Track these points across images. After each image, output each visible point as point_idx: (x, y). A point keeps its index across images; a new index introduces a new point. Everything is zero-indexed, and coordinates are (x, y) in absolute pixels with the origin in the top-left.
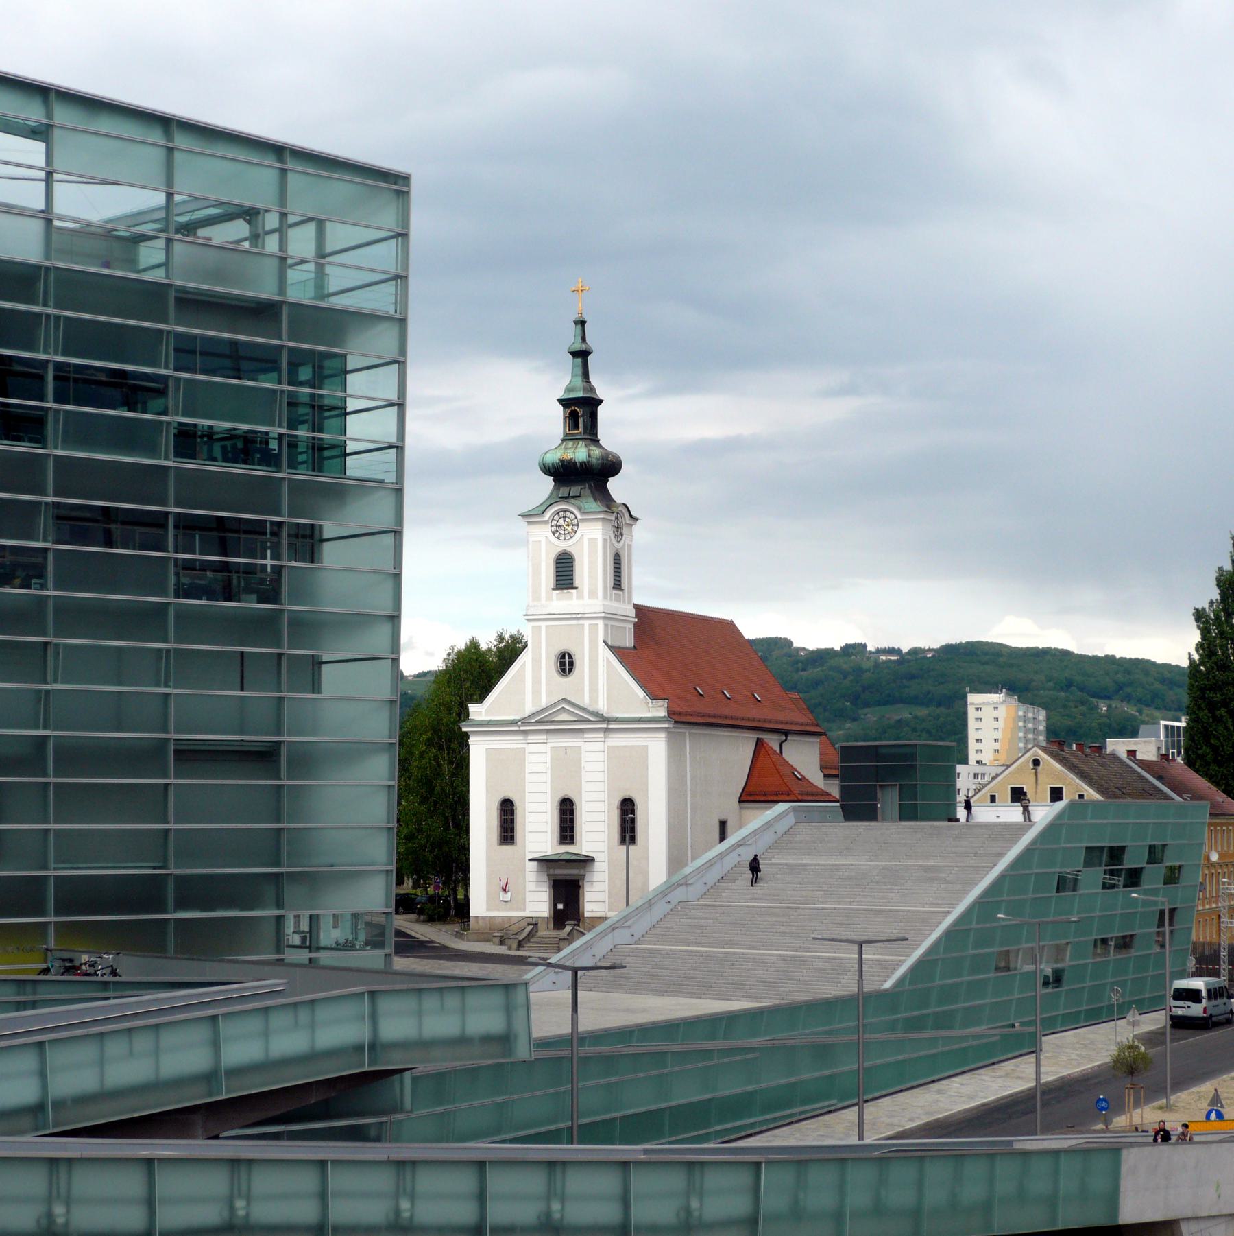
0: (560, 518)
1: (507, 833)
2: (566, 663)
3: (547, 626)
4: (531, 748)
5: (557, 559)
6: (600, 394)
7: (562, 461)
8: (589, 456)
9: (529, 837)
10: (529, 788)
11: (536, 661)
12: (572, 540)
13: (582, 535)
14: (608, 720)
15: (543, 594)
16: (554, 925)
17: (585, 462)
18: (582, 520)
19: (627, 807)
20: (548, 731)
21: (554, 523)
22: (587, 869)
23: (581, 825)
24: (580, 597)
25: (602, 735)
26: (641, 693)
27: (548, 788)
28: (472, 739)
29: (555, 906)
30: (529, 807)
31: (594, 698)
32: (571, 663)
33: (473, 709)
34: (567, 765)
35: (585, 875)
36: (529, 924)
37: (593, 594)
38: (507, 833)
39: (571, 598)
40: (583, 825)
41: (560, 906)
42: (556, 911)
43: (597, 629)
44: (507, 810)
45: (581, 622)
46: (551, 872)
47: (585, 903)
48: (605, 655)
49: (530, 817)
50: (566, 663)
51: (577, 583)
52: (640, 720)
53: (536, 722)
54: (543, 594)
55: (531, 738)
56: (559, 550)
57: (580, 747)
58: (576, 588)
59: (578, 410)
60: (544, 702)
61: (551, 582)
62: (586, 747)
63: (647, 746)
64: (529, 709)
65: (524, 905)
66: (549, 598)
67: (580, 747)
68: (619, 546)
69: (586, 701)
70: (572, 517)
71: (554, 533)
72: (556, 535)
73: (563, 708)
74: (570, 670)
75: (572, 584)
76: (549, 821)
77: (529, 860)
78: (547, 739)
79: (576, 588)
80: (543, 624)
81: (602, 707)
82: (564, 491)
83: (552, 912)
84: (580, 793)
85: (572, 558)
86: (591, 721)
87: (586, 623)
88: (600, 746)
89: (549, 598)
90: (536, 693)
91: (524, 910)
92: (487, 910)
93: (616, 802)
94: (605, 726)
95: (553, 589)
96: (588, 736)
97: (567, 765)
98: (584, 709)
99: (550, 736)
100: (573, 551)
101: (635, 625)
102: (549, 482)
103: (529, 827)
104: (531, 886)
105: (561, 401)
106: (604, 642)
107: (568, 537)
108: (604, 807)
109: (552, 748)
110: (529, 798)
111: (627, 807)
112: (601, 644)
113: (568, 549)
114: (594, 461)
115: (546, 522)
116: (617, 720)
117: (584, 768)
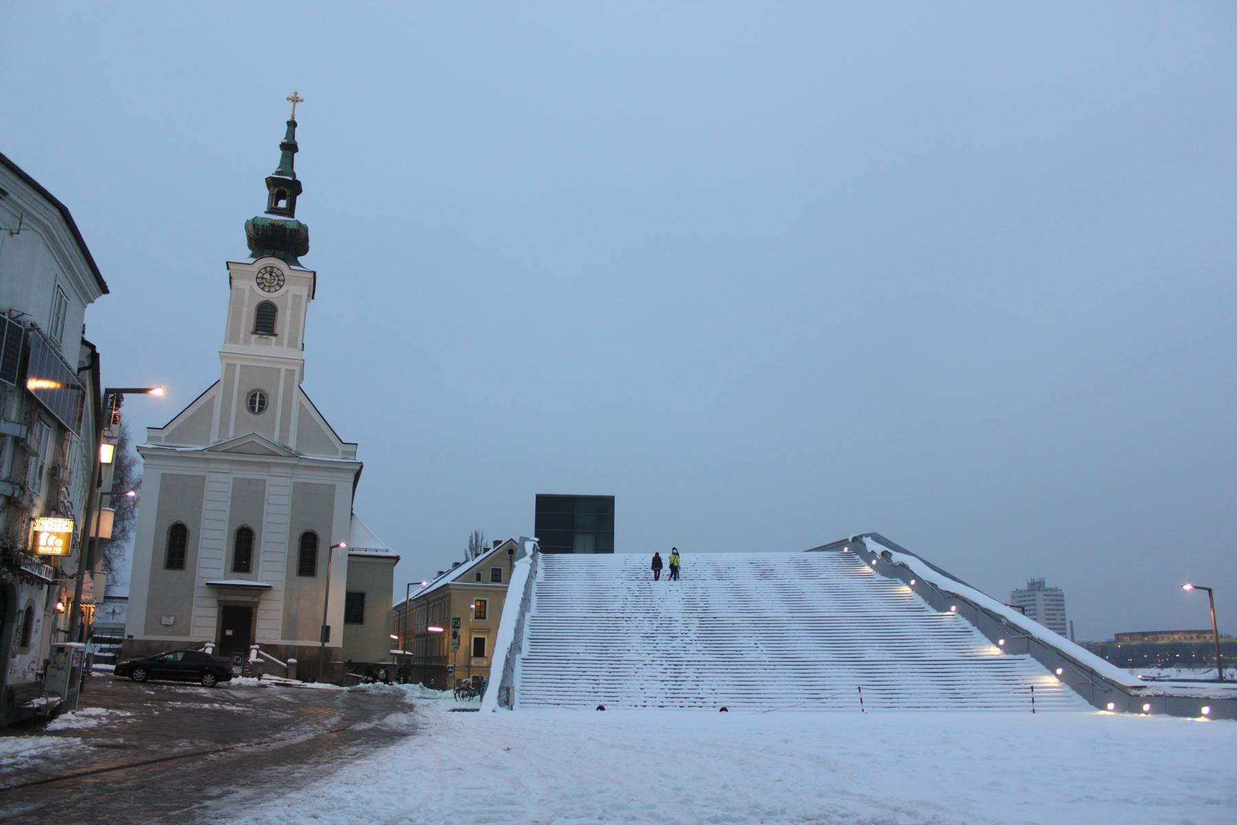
0: (267, 272)
3: (242, 366)
12: (277, 293)
13: (288, 291)
15: (242, 336)
17: (295, 230)
20: (233, 462)
21: (260, 275)
22: (262, 597)
23: (259, 554)
24: (280, 344)
27: (226, 516)
29: (223, 632)
34: (247, 495)
35: (259, 602)
40: (261, 555)
41: (229, 633)
43: (294, 374)
46: (222, 598)
49: (203, 543)
51: (277, 330)
54: (242, 336)
55: (212, 466)
56: (262, 300)
57: (265, 481)
58: (276, 335)
59: (286, 190)
61: (251, 327)
63: (335, 485)
65: (189, 631)
67: (265, 481)
71: (259, 284)
72: (261, 286)
73: (253, 441)
74: (261, 410)
75: (272, 331)
76: (225, 548)
78: (231, 470)
83: (219, 638)
84: (261, 523)
86: (281, 456)
90: (224, 424)
91: (188, 635)
92: (145, 633)
95: (253, 333)
97: (247, 495)
104: (196, 611)
107: (273, 289)
108: (284, 538)
109: (235, 479)
117: (267, 500)
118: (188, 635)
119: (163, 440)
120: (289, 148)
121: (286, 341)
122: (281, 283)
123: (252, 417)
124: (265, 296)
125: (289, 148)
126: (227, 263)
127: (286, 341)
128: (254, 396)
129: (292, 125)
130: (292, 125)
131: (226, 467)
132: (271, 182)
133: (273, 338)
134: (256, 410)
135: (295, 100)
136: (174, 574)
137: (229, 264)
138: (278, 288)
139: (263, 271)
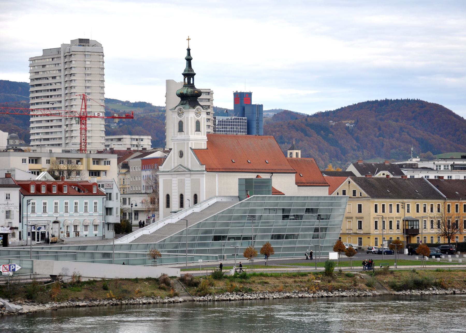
1: (168, 205)
2: (181, 154)
3: (177, 143)
4: (173, 179)
6: (195, 72)
7: (181, 93)
8: (187, 92)
9: (173, 206)
10: (173, 191)
11: (174, 153)
14: (190, 171)
15: (176, 133)
19: (182, 196)
24: (184, 134)
25: (189, 175)
26: (198, 163)
27: (177, 191)
28: (160, 176)
30: (173, 197)
31: (188, 164)
33: (160, 167)
34: (181, 184)
38: (168, 205)
39: (182, 135)
44: (168, 197)
45: (185, 142)
48: (190, 151)
49: (173, 200)
50: (181, 154)
51: (184, 130)
52: (198, 171)
53: (174, 171)
54: (176, 133)
55: (173, 176)
56: (179, 120)
57: (184, 179)
58: (183, 132)
60: (176, 166)
61: (178, 131)
62: (186, 179)
64: (173, 168)
67: (184, 179)
68: (199, 119)
69: (186, 165)
71: (178, 115)
79: (183, 132)
81: (190, 167)
82: (182, 102)
87: (186, 142)
88: (189, 179)
89: (177, 135)
90: (174, 163)
93: (179, 194)
94: (189, 173)
95: (178, 132)
97: (181, 184)
98: (185, 168)
99: (178, 175)
100: (200, 120)
101: (207, 142)
102: (179, 99)
103: (173, 203)
105: (183, 74)
106: (191, 148)
109: (178, 179)
110: (173, 194)
111: (182, 196)
112: (189, 148)
114: (188, 93)
116: (192, 171)
120: (189, 60)
121: (186, 133)
124: (180, 119)
125: (189, 60)
127: (186, 133)
128: (181, 152)
129: (189, 50)
130: (189, 50)
131: (176, 176)
132: (185, 75)
133: (183, 133)
135: (189, 39)
136: (168, 209)
138: (182, 115)
139: (179, 110)
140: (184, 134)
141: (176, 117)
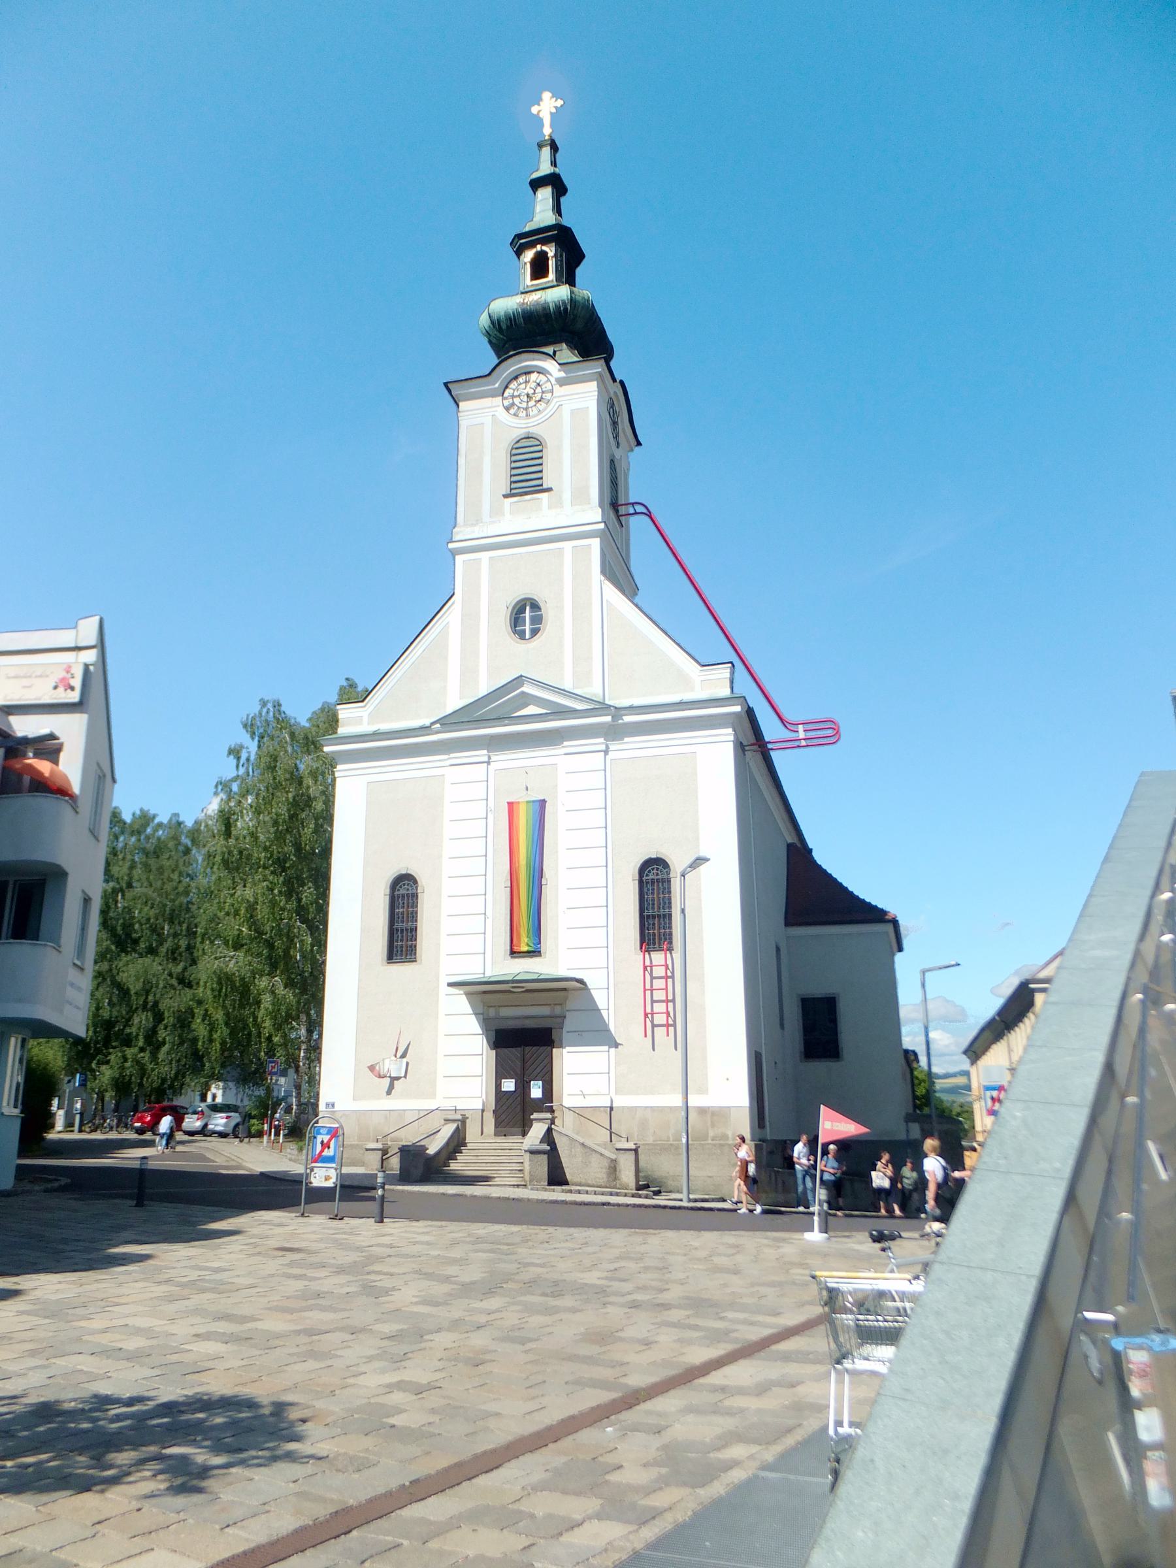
5: (512, 449)
11: (470, 620)
15: (486, 507)
16: (496, 1126)
18: (561, 382)
24: (557, 504)
29: (498, 1086)
32: (537, 620)
36: (447, 1121)
37: (579, 496)
42: (500, 1095)
47: (566, 1077)
54: (486, 507)
58: (549, 490)
61: (504, 488)
64: (454, 702)
66: (497, 512)
70: (542, 378)
71: (507, 409)
72: (512, 411)
74: (535, 632)
77: (450, 985)
80: (485, 556)
85: (541, 444)
87: (568, 546)
90: (468, 673)
91: (433, 1095)
95: (505, 496)
96: (570, 745)
107: (535, 411)
113: (531, 430)
115: (493, 394)
118: (433, 1095)
119: (365, 719)
121: (567, 496)
122: (548, 396)
123: (520, 647)
124: (517, 426)
126: (446, 385)
127: (567, 496)
134: (527, 636)
136: (400, 970)
137: (450, 386)
140: (559, 504)
141: (488, 420)
